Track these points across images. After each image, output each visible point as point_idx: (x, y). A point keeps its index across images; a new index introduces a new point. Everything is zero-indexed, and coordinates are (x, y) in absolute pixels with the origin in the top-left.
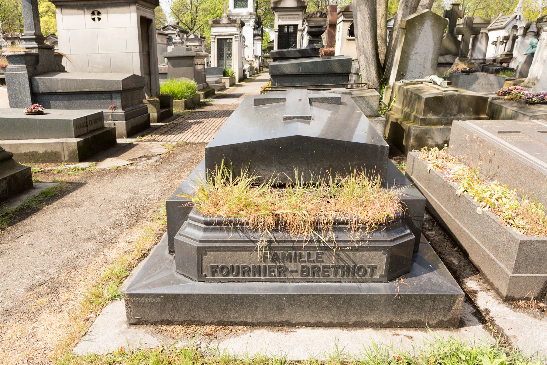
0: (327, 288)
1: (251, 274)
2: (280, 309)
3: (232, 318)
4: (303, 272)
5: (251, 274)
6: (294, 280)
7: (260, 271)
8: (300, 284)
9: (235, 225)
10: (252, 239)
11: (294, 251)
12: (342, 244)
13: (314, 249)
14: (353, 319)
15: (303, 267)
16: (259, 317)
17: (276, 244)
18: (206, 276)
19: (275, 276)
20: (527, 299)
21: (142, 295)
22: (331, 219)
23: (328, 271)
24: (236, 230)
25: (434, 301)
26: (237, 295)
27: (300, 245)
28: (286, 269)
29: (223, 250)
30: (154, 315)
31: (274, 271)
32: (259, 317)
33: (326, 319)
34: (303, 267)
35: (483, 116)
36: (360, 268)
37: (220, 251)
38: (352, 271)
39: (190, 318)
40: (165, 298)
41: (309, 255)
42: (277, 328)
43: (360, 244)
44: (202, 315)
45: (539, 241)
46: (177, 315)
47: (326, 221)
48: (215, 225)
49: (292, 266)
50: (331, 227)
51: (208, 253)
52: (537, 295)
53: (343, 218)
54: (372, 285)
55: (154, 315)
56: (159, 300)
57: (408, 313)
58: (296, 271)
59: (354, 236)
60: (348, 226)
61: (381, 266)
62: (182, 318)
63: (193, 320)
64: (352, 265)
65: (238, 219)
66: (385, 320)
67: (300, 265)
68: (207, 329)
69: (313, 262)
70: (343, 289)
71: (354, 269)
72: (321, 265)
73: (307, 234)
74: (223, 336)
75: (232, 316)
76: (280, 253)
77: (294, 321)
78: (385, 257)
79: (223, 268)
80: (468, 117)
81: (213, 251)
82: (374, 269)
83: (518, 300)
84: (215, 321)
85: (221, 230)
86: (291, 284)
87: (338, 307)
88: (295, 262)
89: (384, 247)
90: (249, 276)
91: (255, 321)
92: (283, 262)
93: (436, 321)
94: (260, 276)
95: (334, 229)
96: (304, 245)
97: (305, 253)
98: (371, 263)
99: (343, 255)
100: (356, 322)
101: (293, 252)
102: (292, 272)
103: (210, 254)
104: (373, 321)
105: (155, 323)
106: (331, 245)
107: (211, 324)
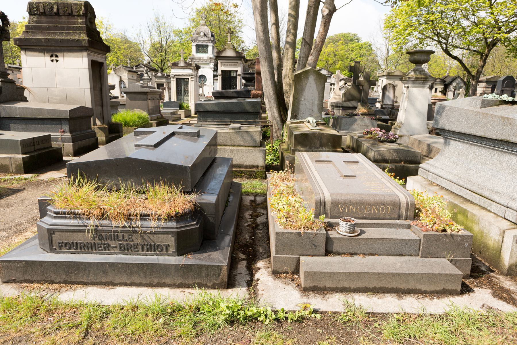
0: (136, 259)
1: (86, 248)
2: (105, 273)
3: (73, 278)
4: (121, 248)
5: (86, 248)
6: (115, 254)
7: (92, 246)
8: (119, 256)
9: (75, 215)
10: (86, 224)
11: (113, 235)
12: (144, 229)
13: (128, 232)
14: (156, 281)
15: (120, 244)
16: (92, 278)
17: (100, 228)
18: (55, 249)
19: (102, 250)
20: (287, 273)
21: (10, 261)
22: (138, 212)
23: (137, 248)
24: (75, 218)
25: (208, 269)
26: (75, 262)
27: (117, 229)
28: (109, 246)
29: (65, 232)
30: (19, 276)
31: (101, 247)
32: (92, 278)
33: (137, 280)
34: (120, 244)
35: (339, 150)
36: (158, 246)
37: (63, 232)
38: (153, 248)
39: (44, 278)
40: (26, 263)
41: (123, 236)
42: (104, 286)
43: (156, 229)
44: (53, 277)
45: (289, 233)
46: (35, 276)
47: (135, 214)
48: (61, 214)
49: (113, 244)
50: (138, 217)
51: (56, 233)
52: (293, 270)
53: (147, 212)
54: (166, 257)
55: (19, 276)
56: (21, 265)
57: (192, 278)
58: (116, 247)
59: (153, 224)
60: (151, 218)
61: (172, 245)
62: (39, 278)
63: (46, 279)
64: (152, 243)
65: (77, 211)
66: (178, 282)
67: (118, 243)
68: (56, 286)
69: (127, 241)
70: (148, 260)
71: (154, 247)
72: (132, 243)
73: (120, 223)
74: (64, 290)
75: (73, 278)
76: (103, 234)
77: (116, 282)
78: (173, 239)
79: (66, 244)
80: (327, 149)
81: (59, 232)
82: (167, 247)
83: (281, 273)
84: (62, 281)
85: (66, 218)
86: (113, 256)
87: (144, 272)
88: (115, 240)
89: (172, 232)
90: (85, 250)
91: (89, 281)
92: (107, 240)
93: (211, 284)
94: (92, 250)
95: (141, 219)
96: (120, 229)
97: (120, 235)
98: (164, 242)
99: (145, 237)
100: (158, 283)
101: (112, 234)
102: (113, 247)
103: (57, 234)
104: (169, 283)
105: (20, 282)
106: (137, 229)
107: (59, 283)
